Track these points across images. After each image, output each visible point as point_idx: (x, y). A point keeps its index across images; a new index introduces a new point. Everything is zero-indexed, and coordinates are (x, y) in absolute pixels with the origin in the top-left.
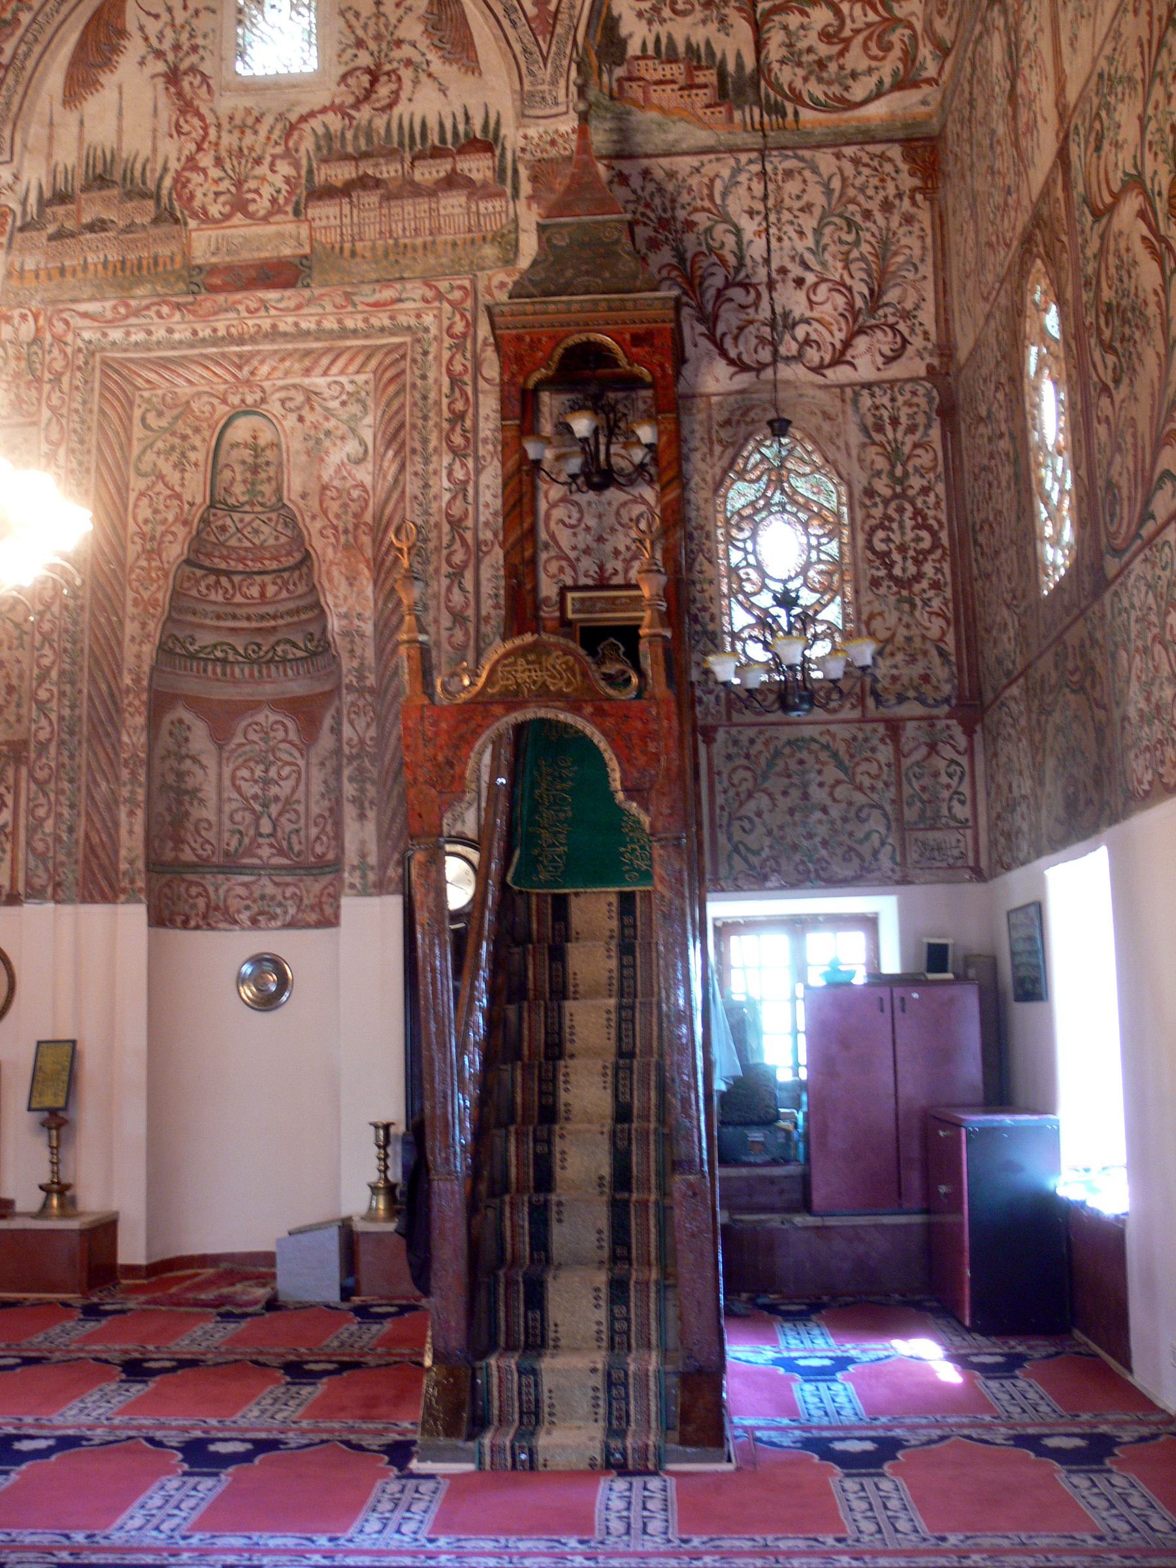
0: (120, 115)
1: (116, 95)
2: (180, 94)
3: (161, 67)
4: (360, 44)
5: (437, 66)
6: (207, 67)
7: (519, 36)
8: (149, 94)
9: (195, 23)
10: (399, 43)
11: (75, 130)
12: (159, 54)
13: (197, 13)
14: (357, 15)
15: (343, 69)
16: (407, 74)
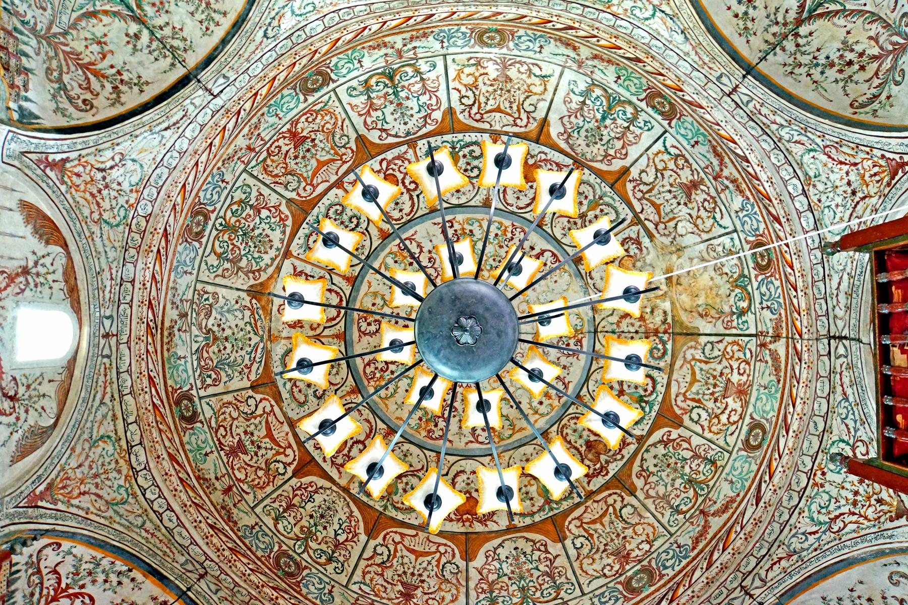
0: (12, 236)
1: (21, 234)
2: (17, 275)
3: (31, 264)
4: (28, 387)
5: (16, 436)
6: (28, 293)
7: (27, 488)
8: (17, 255)
9: (47, 286)
10: (27, 411)
11: (8, 205)
12: (36, 264)
13: (51, 288)
14: (40, 384)
15: (18, 378)
16: (12, 419)
